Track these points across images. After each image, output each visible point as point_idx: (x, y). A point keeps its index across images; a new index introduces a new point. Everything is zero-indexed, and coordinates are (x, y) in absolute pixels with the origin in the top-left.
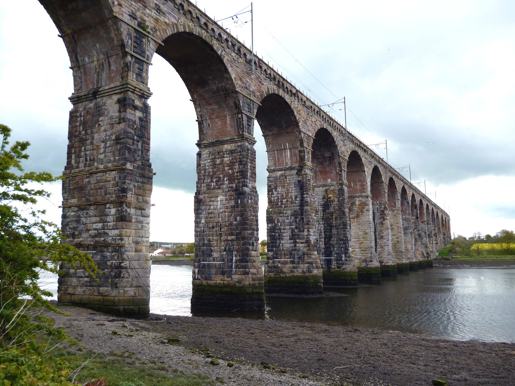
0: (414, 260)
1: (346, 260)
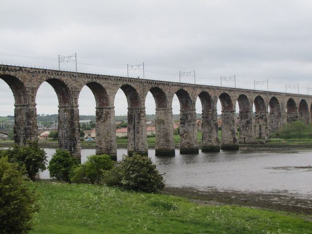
0: (195, 146)
1: (74, 151)
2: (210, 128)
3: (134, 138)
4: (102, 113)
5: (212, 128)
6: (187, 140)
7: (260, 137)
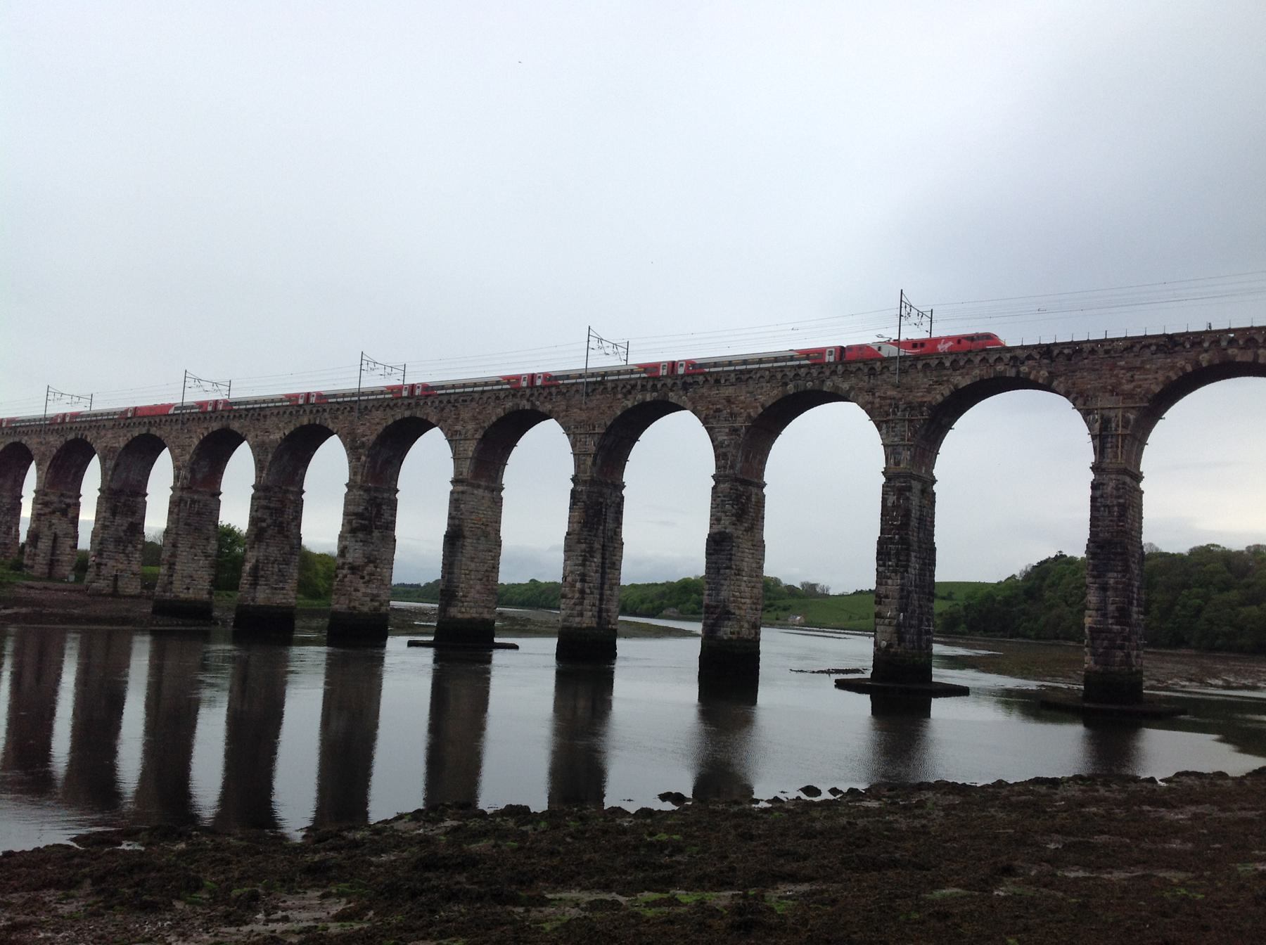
2: (287, 548)
3: (603, 584)
4: (749, 498)
5: (292, 548)
6: (373, 589)
7: (50, 576)
